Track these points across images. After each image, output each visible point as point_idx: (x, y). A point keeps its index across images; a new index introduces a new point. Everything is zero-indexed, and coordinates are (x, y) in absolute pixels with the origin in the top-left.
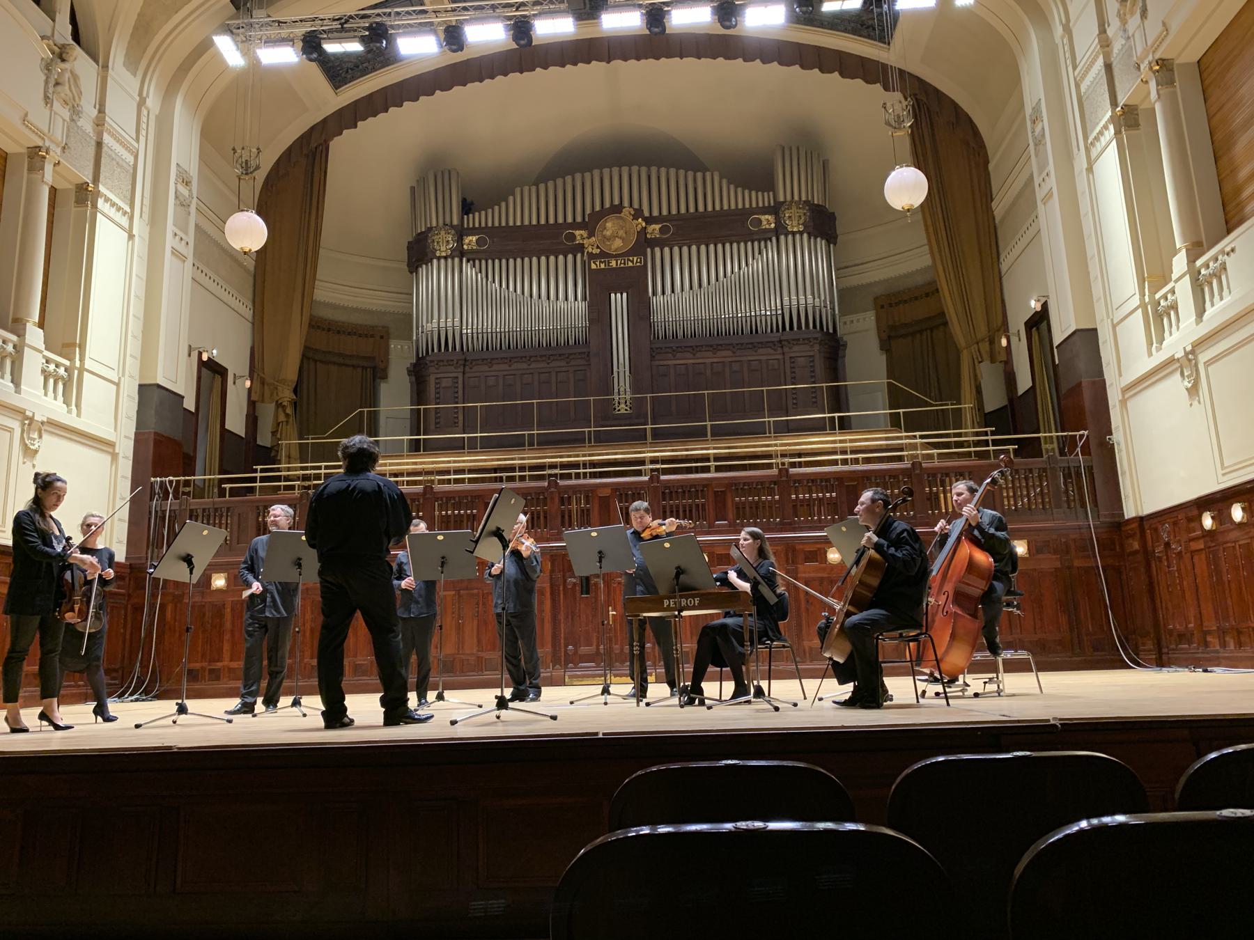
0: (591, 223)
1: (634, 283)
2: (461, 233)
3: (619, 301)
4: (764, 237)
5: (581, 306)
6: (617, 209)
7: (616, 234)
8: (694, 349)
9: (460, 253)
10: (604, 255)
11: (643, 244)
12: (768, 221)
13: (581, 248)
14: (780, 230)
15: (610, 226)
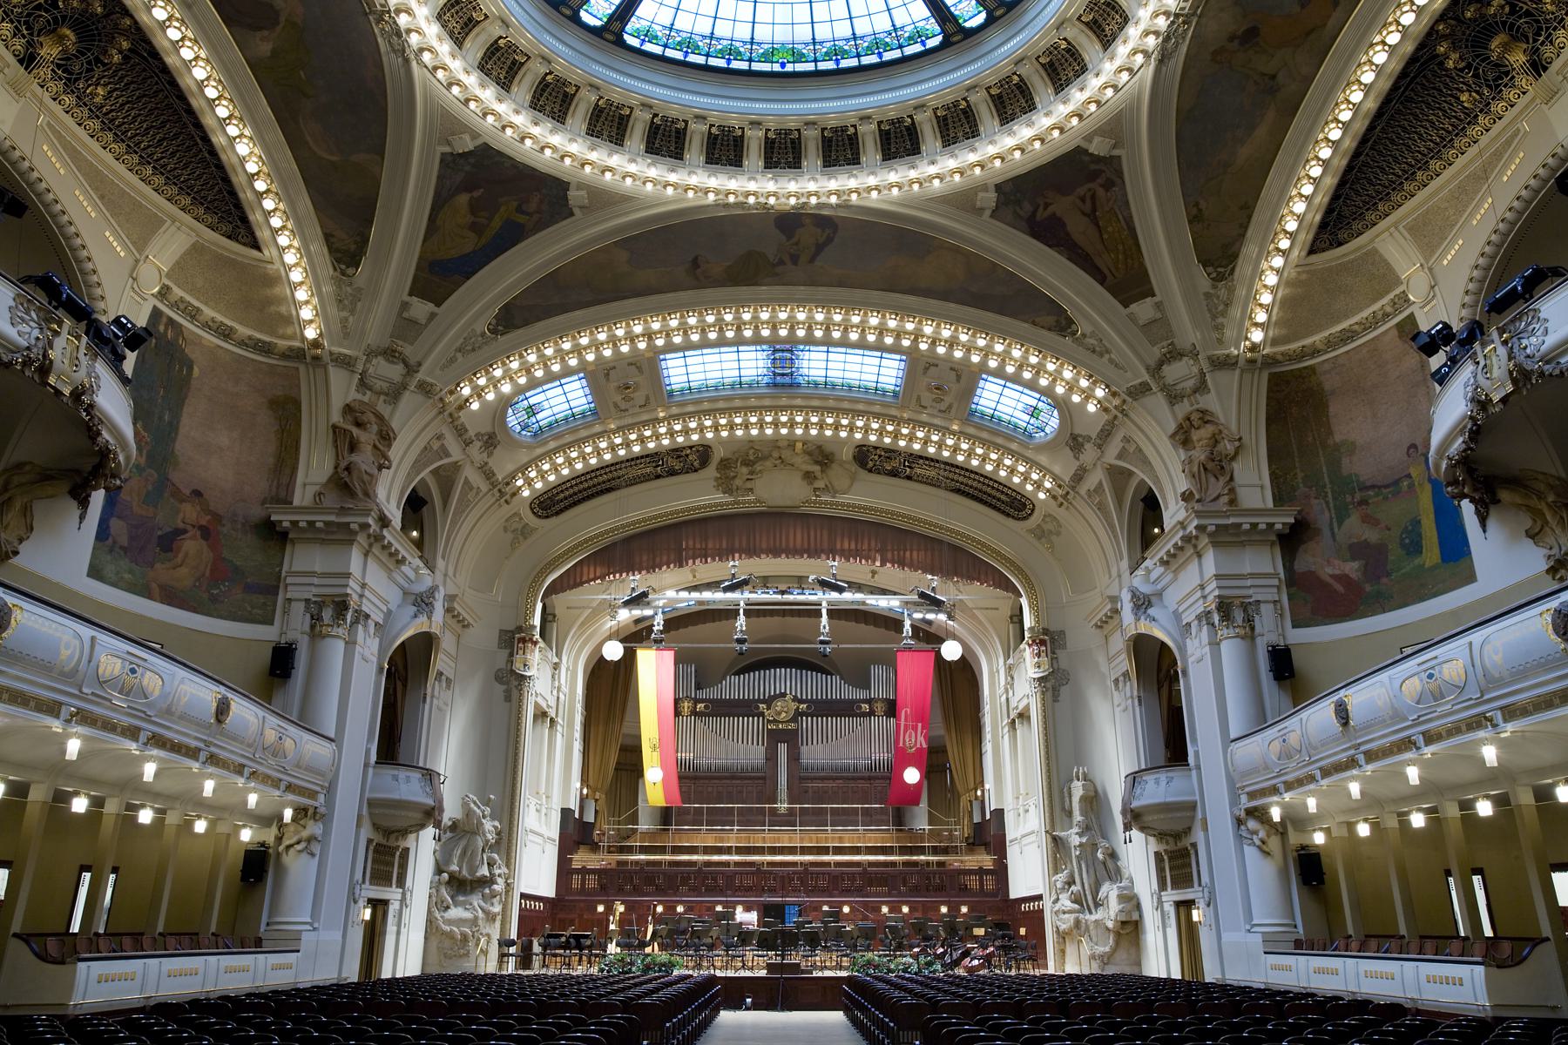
0: (769, 701)
1: (791, 738)
2: (697, 701)
3: (783, 749)
4: (864, 715)
5: (761, 749)
6: (783, 695)
7: (783, 710)
8: (823, 779)
9: (694, 713)
10: (775, 721)
11: (798, 714)
12: (865, 707)
13: (762, 714)
14: (872, 713)
15: (779, 704)
